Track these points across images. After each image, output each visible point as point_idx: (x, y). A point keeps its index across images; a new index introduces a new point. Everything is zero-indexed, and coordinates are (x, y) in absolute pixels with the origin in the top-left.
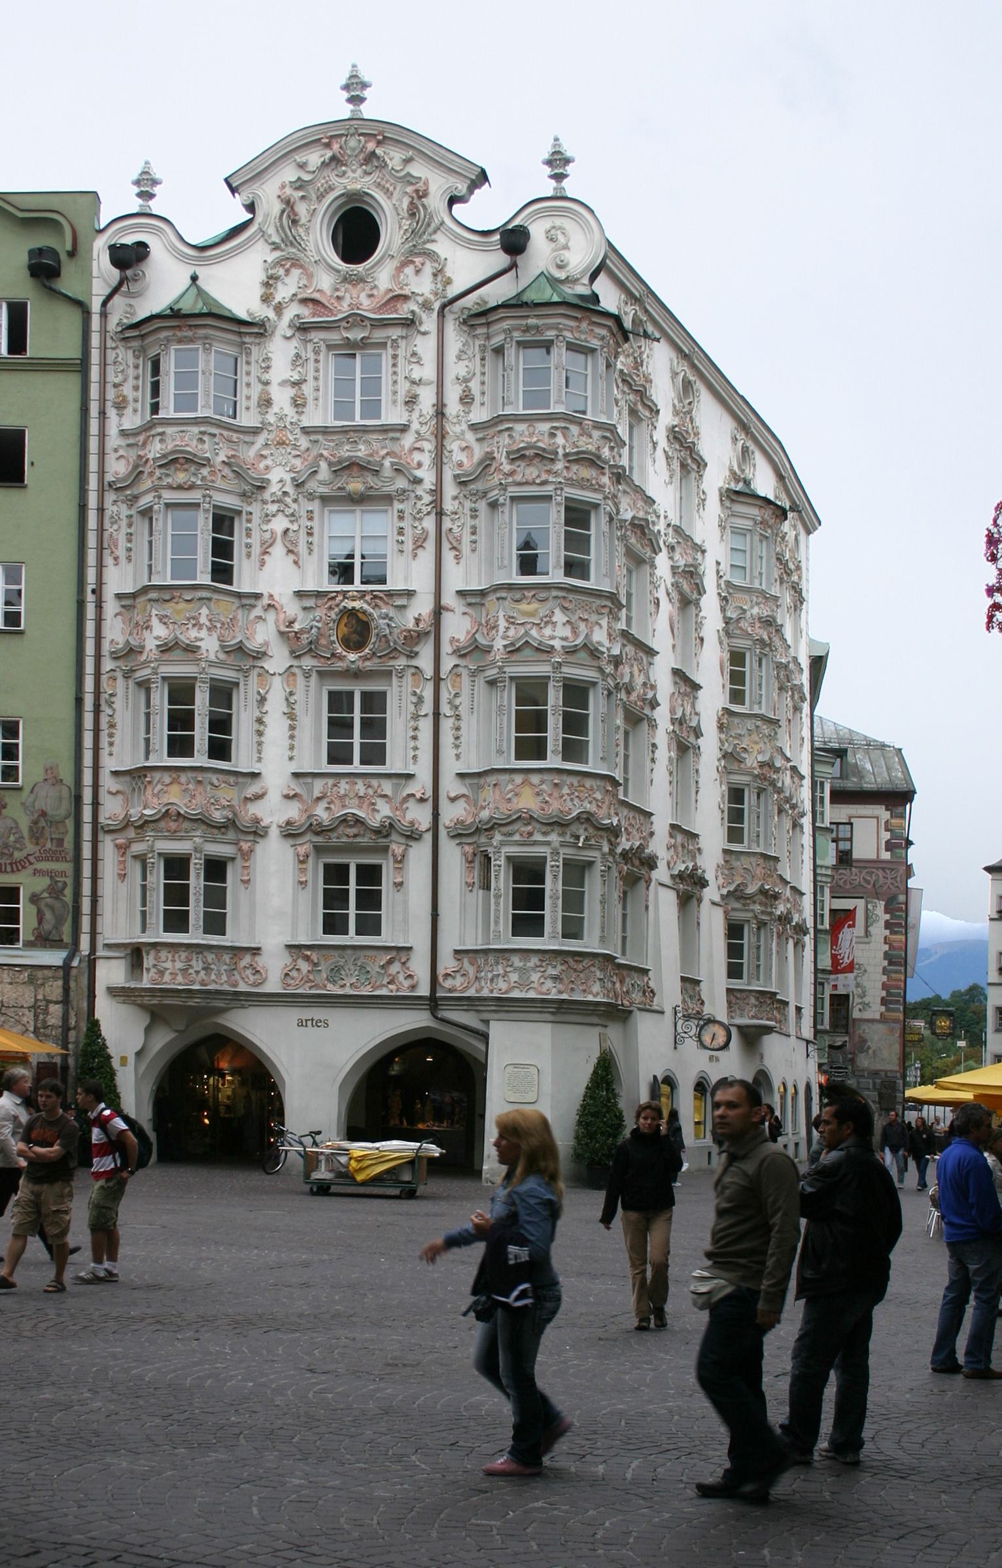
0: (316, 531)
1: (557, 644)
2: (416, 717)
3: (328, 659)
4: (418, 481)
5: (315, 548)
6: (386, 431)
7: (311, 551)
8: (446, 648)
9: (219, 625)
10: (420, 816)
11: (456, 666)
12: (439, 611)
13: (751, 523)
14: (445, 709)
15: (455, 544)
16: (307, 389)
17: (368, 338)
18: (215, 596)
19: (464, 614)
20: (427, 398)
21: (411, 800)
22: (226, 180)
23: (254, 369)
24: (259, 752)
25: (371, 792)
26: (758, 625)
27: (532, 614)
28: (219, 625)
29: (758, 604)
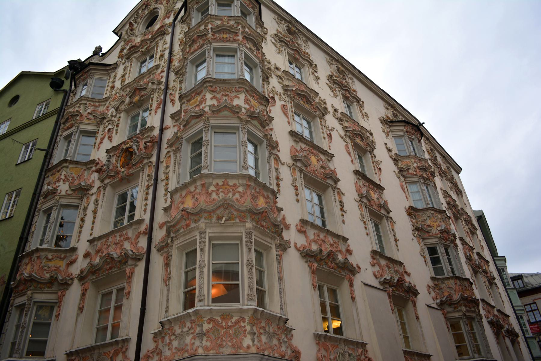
0: (120, 125)
1: (207, 109)
2: (148, 187)
3: (114, 176)
4: (160, 83)
5: (119, 132)
6: (150, 72)
7: (117, 133)
8: (164, 145)
9: (70, 179)
10: (143, 243)
11: (169, 152)
12: (162, 130)
13: (402, 133)
14: (161, 176)
15: (172, 98)
16: (127, 76)
17: (149, 47)
18: (70, 166)
19: (174, 126)
20: (167, 53)
21: (141, 236)
22: (114, 31)
23: (112, 79)
24: (79, 237)
25: (122, 238)
26: (418, 170)
27: (195, 103)
28: (70, 179)
29: (415, 162)
